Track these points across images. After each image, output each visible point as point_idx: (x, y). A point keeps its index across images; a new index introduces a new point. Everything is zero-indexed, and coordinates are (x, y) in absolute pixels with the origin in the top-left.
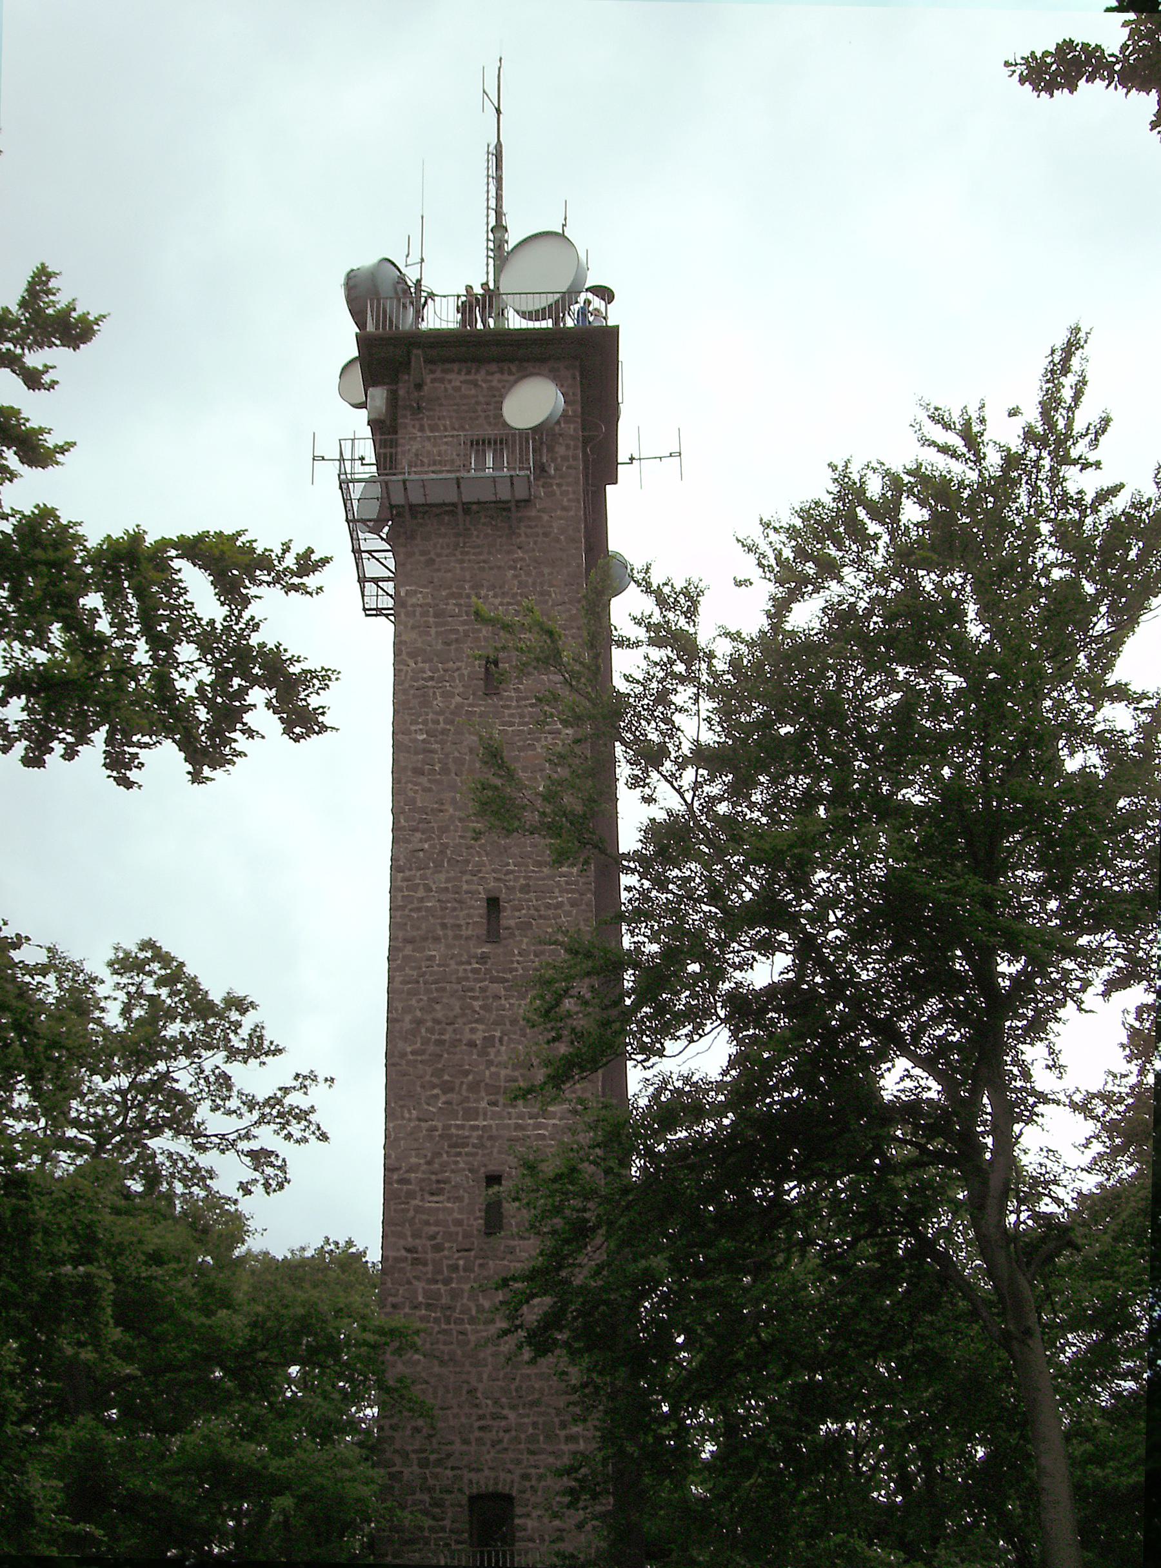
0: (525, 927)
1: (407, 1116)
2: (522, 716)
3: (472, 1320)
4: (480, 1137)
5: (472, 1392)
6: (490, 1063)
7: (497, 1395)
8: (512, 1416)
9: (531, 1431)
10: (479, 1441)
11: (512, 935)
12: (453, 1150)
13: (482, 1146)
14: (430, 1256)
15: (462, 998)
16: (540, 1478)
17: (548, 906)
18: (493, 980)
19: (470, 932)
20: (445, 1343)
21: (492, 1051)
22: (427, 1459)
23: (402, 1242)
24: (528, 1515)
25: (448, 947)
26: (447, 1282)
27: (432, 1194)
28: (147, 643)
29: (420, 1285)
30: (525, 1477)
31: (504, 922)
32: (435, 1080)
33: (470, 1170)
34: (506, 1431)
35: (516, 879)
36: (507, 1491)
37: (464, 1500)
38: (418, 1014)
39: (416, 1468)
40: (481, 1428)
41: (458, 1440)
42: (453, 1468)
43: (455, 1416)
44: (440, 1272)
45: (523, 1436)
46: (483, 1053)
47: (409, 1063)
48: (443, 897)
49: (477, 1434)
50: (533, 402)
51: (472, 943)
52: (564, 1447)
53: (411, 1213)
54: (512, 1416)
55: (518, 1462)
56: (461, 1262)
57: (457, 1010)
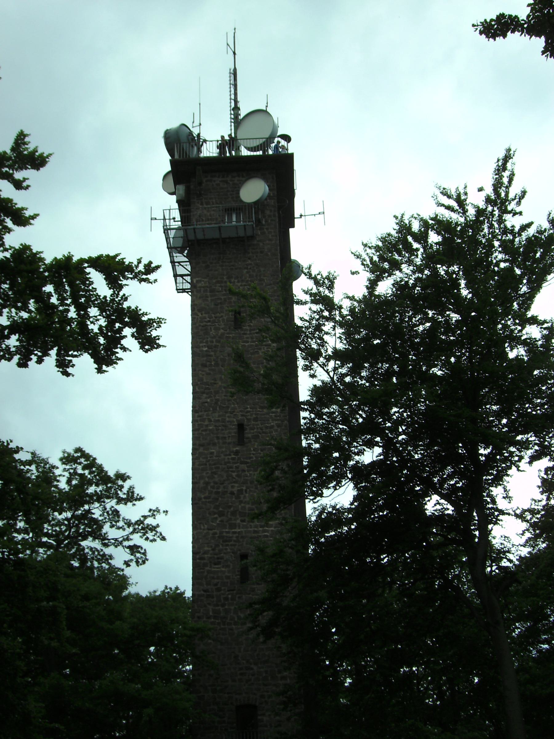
0: (256, 437)
1: (202, 527)
2: (252, 338)
4: (237, 537)
8: (255, 668)
9: (264, 675)
17: (267, 427)
18: (242, 463)
19: (230, 440)
21: (242, 496)
26: (223, 605)
27: (215, 564)
28: (75, 308)
29: (210, 608)
31: (246, 435)
32: (215, 510)
33: (233, 553)
35: (251, 415)
38: (207, 479)
40: (241, 674)
50: (254, 190)
53: (206, 574)
54: (255, 668)
56: (230, 596)
57: (225, 477)
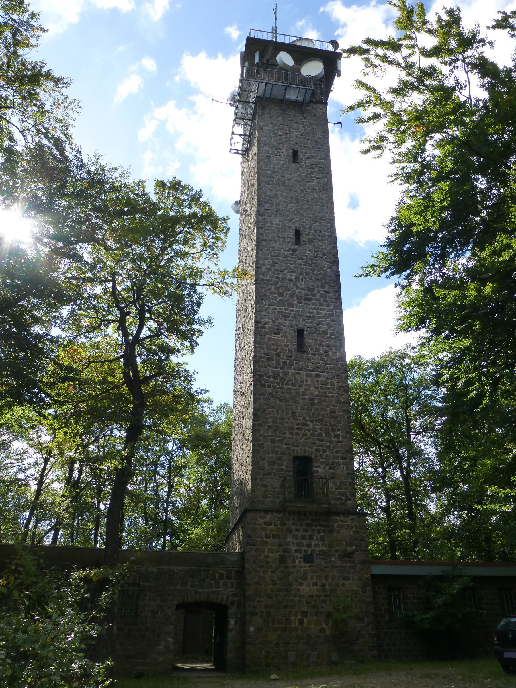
0: (310, 242)
1: (264, 303)
2: (307, 171)
3: (293, 385)
4: (295, 314)
5: (294, 413)
6: (298, 288)
7: (304, 415)
8: (311, 425)
9: (319, 431)
10: (297, 434)
11: (305, 244)
12: (284, 318)
13: (296, 318)
14: (274, 357)
15: (285, 263)
16: (324, 451)
17: (319, 236)
18: (299, 259)
19: (289, 240)
20: (282, 393)
21: (299, 284)
22: (274, 439)
23: (263, 351)
24: (319, 467)
25: (280, 244)
26: (282, 368)
27: (275, 334)
28: (195, 54)
29: (271, 369)
30: (318, 450)
31: (302, 239)
32: (276, 291)
33: (291, 326)
34: (309, 431)
35: (307, 225)
36: (309, 455)
37: (291, 459)
38: (269, 266)
39: (269, 443)
40: (298, 429)
41: (287, 432)
42: (286, 444)
43: (287, 423)
44: (280, 364)
45: (316, 433)
46: (295, 284)
47: (265, 283)
48: (278, 227)
49: (296, 431)
50: (313, 69)
51: (290, 244)
52: (333, 439)
53: (266, 340)
54: (311, 425)
55: (314, 444)
56: (288, 361)
57: (284, 267)
